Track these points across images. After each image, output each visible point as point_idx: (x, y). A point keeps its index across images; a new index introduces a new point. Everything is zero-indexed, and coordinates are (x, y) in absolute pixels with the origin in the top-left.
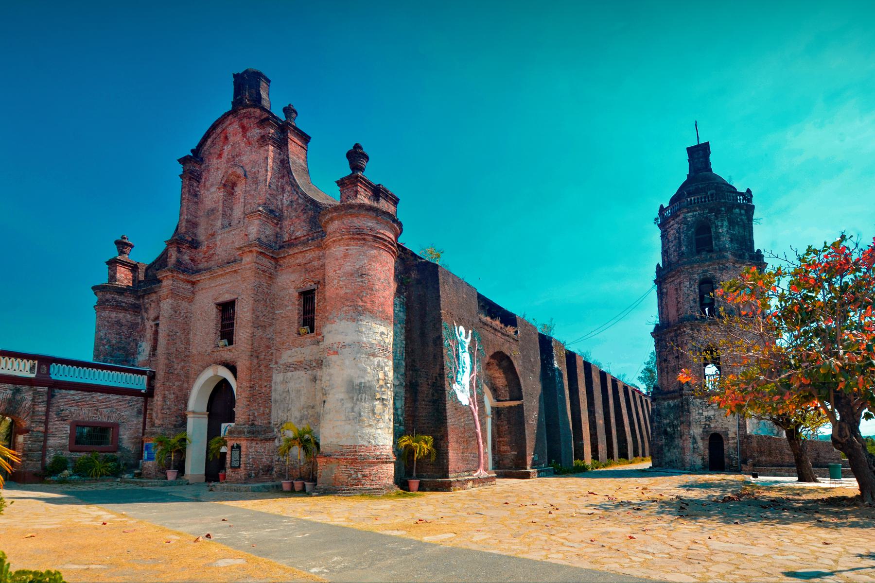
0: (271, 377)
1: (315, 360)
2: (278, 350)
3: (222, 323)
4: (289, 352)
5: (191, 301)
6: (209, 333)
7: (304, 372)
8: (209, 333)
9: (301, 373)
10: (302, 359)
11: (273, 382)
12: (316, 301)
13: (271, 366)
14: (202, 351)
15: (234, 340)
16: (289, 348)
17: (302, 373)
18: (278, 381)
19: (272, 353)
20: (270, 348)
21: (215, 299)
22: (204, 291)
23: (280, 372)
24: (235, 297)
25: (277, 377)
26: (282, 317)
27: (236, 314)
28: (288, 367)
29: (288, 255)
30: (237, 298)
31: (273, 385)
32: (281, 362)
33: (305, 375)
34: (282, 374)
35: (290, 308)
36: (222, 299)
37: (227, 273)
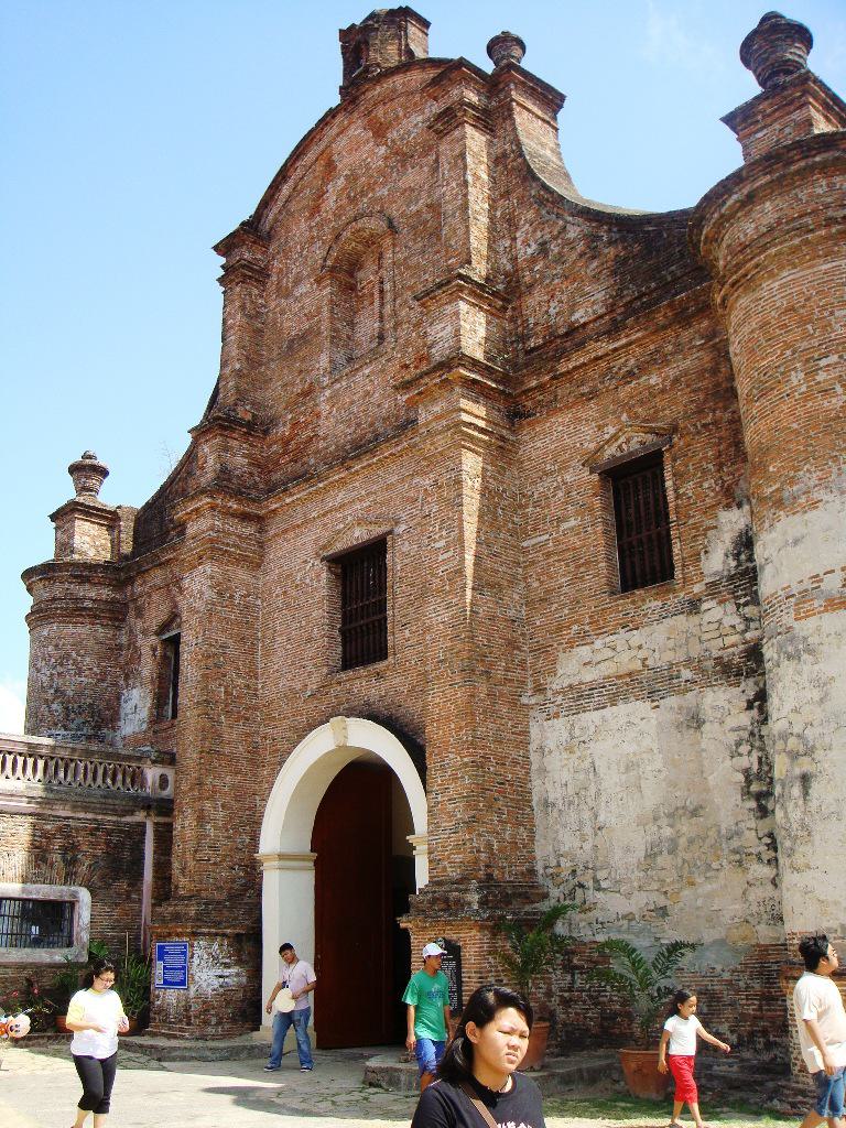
0: (526, 733)
1: (689, 661)
2: (542, 650)
3: (343, 606)
4: (584, 652)
5: (256, 564)
7: (648, 704)
8: (309, 640)
9: (636, 710)
10: (638, 665)
11: (532, 747)
12: (669, 484)
13: (524, 700)
14: (291, 689)
15: (390, 644)
16: (583, 638)
17: (642, 708)
18: (551, 744)
19: (523, 662)
20: (518, 648)
21: (324, 547)
22: (291, 535)
23: (557, 716)
24: (377, 531)
25: (549, 733)
26: (548, 555)
27: (389, 574)
28: (580, 697)
30: (391, 532)
31: (534, 757)
32: (556, 684)
33: (653, 714)
34: (561, 720)
35: (572, 523)
36: (339, 546)
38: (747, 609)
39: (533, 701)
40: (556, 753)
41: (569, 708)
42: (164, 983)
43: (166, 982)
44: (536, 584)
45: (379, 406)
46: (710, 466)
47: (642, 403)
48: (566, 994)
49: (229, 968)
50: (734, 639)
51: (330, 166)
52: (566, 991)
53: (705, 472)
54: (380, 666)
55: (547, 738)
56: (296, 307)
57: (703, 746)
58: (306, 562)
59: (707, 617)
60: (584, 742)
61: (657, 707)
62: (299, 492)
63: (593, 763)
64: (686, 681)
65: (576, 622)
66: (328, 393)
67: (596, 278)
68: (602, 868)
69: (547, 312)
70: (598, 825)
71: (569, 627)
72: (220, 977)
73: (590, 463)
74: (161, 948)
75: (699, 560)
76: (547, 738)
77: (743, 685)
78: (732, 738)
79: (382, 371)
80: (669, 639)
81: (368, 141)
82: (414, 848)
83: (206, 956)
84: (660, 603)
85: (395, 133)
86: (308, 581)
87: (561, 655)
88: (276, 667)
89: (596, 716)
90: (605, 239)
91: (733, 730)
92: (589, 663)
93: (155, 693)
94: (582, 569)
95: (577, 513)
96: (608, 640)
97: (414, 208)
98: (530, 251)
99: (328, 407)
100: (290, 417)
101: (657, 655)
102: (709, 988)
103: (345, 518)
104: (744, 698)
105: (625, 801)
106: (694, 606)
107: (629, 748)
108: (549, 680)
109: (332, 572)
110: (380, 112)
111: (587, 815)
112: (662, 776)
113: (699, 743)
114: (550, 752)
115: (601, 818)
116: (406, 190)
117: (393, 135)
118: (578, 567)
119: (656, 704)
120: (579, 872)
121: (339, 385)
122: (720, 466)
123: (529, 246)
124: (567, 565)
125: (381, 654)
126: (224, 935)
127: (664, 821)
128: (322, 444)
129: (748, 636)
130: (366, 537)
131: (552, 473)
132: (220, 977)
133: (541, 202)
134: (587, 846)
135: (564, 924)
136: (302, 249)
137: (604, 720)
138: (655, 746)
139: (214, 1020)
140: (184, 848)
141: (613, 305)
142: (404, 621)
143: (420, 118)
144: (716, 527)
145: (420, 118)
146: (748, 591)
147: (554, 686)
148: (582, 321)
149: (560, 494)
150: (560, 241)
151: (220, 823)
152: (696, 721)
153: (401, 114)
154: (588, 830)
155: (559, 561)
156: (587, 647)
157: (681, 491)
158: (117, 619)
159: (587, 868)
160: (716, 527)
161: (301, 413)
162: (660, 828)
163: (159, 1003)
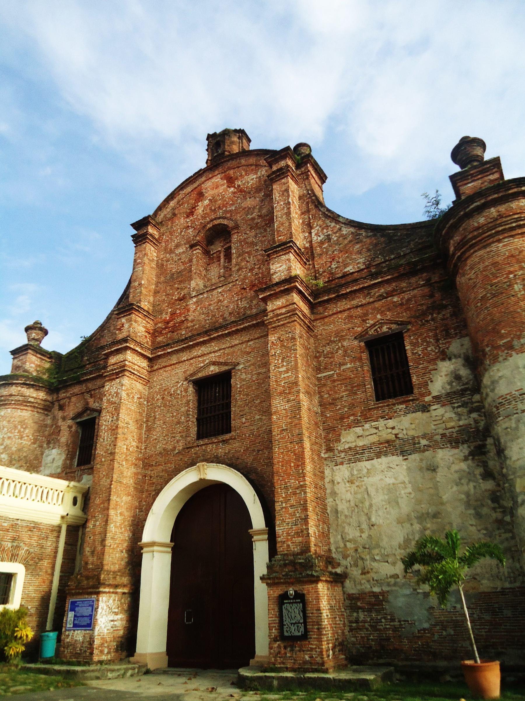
4: (358, 430)
6: (179, 423)
7: (401, 458)
8: (179, 423)
11: (327, 480)
16: (357, 423)
17: (396, 460)
18: (338, 479)
21: (191, 375)
23: (342, 463)
24: (224, 368)
26: (334, 381)
27: (233, 389)
29: (338, 296)
33: (404, 463)
34: (345, 466)
35: (349, 366)
36: (200, 375)
37: (214, 338)
38: (459, 410)
39: (326, 456)
40: (342, 485)
41: (350, 460)
42: (73, 627)
43: (75, 626)
44: (326, 396)
45: (227, 307)
46: (431, 340)
47: (389, 310)
48: (354, 625)
49: (117, 615)
50: (452, 424)
51: (201, 195)
52: (354, 623)
53: (428, 343)
54: (227, 436)
55: (336, 475)
56: (176, 258)
57: (438, 479)
58: (178, 382)
59: (434, 413)
60: (361, 477)
61: (407, 459)
62: (177, 346)
63: (367, 488)
64: (424, 446)
65: (353, 415)
66: (195, 300)
67: (360, 252)
68: (375, 548)
69: (330, 267)
70: (371, 523)
71: (348, 418)
72: (112, 621)
73: (359, 337)
74: (73, 603)
75: (427, 385)
76: (336, 475)
77: (461, 448)
78: (456, 476)
79: (229, 290)
80: (411, 424)
81: (223, 185)
82: (253, 537)
83: (105, 608)
84: (404, 406)
85: (240, 182)
86: (179, 392)
87: (343, 432)
88: (155, 437)
89: (368, 464)
90: (364, 235)
91: (456, 472)
92: (361, 436)
93: (69, 452)
94: (355, 389)
95: (351, 362)
96: (373, 424)
97: (250, 217)
98: (319, 238)
99: (194, 307)
100: (170, 310)
101: (405, 432)
102: (454, 618)
103: (205, 360)
104: (462, 454)
105: (388, 510)
106: (425, 408)
107: (390, 481)
108: (336, 445)
109: (194, 388)
110: (231, 172)
111: (363, 518)
112: (412, 496)
113: (435, 478)
114: (338, 483)
115: (373, 519)
116: (245, 208)
117: (238, 183)
118: (352, 387)
119: (406, 457)
120: (359, 550)
121: (202, 296)
122: (437, 340)
123: (319, 236)
124: (346, 386)
125: (228, 430)
126: (116, 593)
127: (415, 521)
128: (190, 324)
129: (461, 423)
130: (217, 371)
131: (334, 342)
132: (112, 621)
133: (326, 216)
134: (364, 536)
135: (350, 581)
136: (181, 232)
137: (373, 465)
138: (406, 480)
139: (106, 650)
140: (94, 541)
141: (370, 264)
142: (242, 414)
143: (255, 176)
144: (436, 369)
145: (255, 176)
146: (459, 401)
147: (339, 448)
148: (351, 271)
149: (340, 352)
150: (337, 235)
151: (118, 524)
152: (433, 469)
153: (243, 173)
154: (365, 526)
155: (341, 384)
156: (360, 428)
157: (415, 352)
158: (46, 410)
159: (365, 548)
160: (436, 369)
161: (177, 309)
162: (412, 525)
163: (68, 640)
